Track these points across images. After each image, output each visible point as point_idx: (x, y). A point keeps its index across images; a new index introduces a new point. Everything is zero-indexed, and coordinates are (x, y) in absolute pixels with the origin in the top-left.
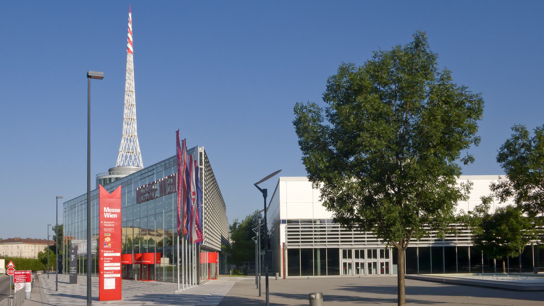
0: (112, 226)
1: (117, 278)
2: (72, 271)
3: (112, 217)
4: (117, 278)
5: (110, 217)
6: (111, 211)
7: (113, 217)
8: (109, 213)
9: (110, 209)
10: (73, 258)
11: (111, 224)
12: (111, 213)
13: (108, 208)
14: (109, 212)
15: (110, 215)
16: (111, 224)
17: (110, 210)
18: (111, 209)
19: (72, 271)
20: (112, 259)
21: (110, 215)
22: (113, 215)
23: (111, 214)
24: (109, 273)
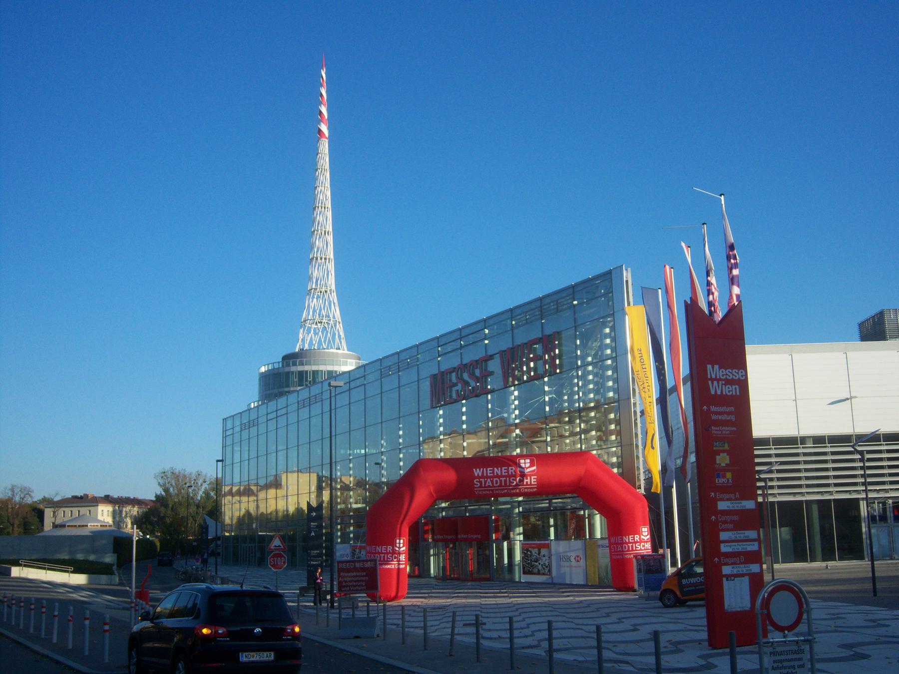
0: (731, 420)
3: (728, 394)
5: (724, 393)
6: (725, 377)
7: (731, 393)
8: (720, 382)
9: (721, 370)
11: (729, 413)
12: (724, 382)
13: (716, 367)
15: (724, 386)
16: (729, 413)
18: (724, 370)
21: (724, 386)
23: (725, 385)
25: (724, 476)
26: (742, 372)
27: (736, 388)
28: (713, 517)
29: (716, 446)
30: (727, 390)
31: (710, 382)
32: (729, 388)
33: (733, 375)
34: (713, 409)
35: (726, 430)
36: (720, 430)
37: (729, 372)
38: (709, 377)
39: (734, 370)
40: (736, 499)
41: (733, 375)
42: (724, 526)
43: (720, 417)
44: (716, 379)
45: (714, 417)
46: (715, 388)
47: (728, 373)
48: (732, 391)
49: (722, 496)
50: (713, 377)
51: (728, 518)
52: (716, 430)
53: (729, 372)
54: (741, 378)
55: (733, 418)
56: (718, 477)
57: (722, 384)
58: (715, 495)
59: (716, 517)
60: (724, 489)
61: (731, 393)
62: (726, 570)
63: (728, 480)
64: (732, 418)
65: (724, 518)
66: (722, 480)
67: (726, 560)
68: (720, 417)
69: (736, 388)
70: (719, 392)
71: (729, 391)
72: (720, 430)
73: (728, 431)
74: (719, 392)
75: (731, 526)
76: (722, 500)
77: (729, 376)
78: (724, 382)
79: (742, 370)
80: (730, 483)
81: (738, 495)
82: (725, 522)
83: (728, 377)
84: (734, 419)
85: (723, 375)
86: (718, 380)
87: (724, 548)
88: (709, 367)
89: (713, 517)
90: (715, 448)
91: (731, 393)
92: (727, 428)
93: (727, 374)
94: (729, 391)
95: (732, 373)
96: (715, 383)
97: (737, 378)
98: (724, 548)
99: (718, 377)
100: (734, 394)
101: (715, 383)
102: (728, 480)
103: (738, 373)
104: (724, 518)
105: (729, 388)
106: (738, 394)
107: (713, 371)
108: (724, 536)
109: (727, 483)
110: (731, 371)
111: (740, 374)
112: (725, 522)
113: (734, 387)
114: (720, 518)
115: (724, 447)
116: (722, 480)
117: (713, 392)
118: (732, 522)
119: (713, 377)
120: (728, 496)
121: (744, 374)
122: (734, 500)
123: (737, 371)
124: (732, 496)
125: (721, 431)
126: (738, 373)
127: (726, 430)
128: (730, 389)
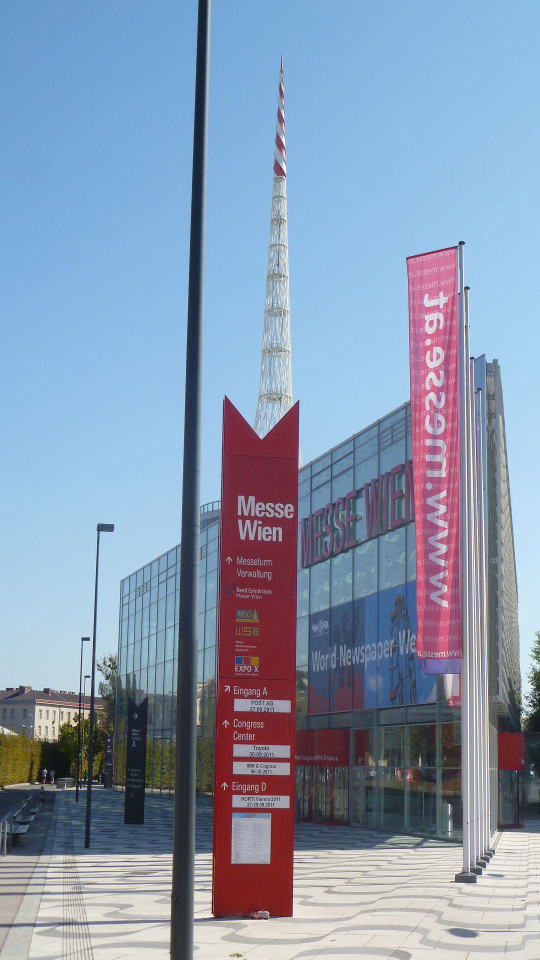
1: (277, 815)
2: (132, 780)
4: (277, 815)
5: (259, 539)
7: (269, 539)
8: (256, 522)
10: (136, 739)
11: (263, 569)
12: (260, 522)
13: (252, 499)
14: (256, 518)
15: (260, 528)
17: (258, 509)
19: (132, 780)
20: (260, 725)
21: (260, 528)
22: (269, 528)
23: (263, 526)
24: (250, 787)
25: (247, 662)
26: (289, 508)
27: (277, 531)
28: (226, 722)
29: (240, 617)
30: (265, 533)
31: (240, 522)
32: (267, 531)
33: (276, 511)
34: (241, 561)
35: (257, 593)
36: (247, 594)
37: (270, 506)
38: (239, 513)
39: (278, 505)
40: (263, 697)
41: (276, 511)
42: (240, 737)
43: (250, 574)
44: (250, 517)
45: (242, 574)
46: (246, 531)
47: (277, 509)
48: (272, 535)
49: (241, 691)
50: (246, 514)
51: (248, 725)
52: (242, 593)
53: (270, 506)
54: (287, 516)
55: (269, 576)
56: (239, 662)
57: (258, 525)
58: (232, 689)
59: (231, 723)
60: (247, 682)
61: (270, 538)
62: (237, 801)
63: (253, 668)
64: (268, 575)
65: (241, 724)
66: (244, 668)
67: (239, 787)
68: (250, 574)
69: (277, 531)
70: (252, 538)
71: (267, 536)
72: (247, 594)
73: (258, 594)
74: (252, 538)
75: (252, 737)
76: (241, 697)
77: (270, 513)
78: (260, 522)
79: (291, 505)
80: (256, 673)
81: (265, 692)
82: (243, 730)
83: (267, 514)
84: (270, 578)
85: (260, 512)
86: (252, 519)
87: (239, 768)
88: (241, 498)
89: (226, 722)
90: (237, 620)
91: (270, 538)
92: (259, 591)
93: (266, 511)
94: (267, 536)
95: (274, 509)
96: (248, 522)
97: (281, 516)
98: (239, 768)
99: (253, 514)
100: (274, 540)
101: (248, 522)
102: (253, 668)
103: (283, 509)
104: (241, 724)
105: (267, 531)
106: (280, 540)
107: (247, 505)
108: (239, 750)
109: (253, 672)
110: (273, 506)
111: (286, 510)
112: (243, 730)
113: (275, 529)
114: (236, 723)
115: (252, 618)
116: (244, 668)
117: (243, 537)
118: (252, 731)
119: (246, 514)
120: (251, 692)
121: (292, 510)
122: (258, 698)
123: (282, 506)
124: (257, 692)
125: (249, 594)
126: (283, 509)
127: (257, 593)
128: (270, 533)
